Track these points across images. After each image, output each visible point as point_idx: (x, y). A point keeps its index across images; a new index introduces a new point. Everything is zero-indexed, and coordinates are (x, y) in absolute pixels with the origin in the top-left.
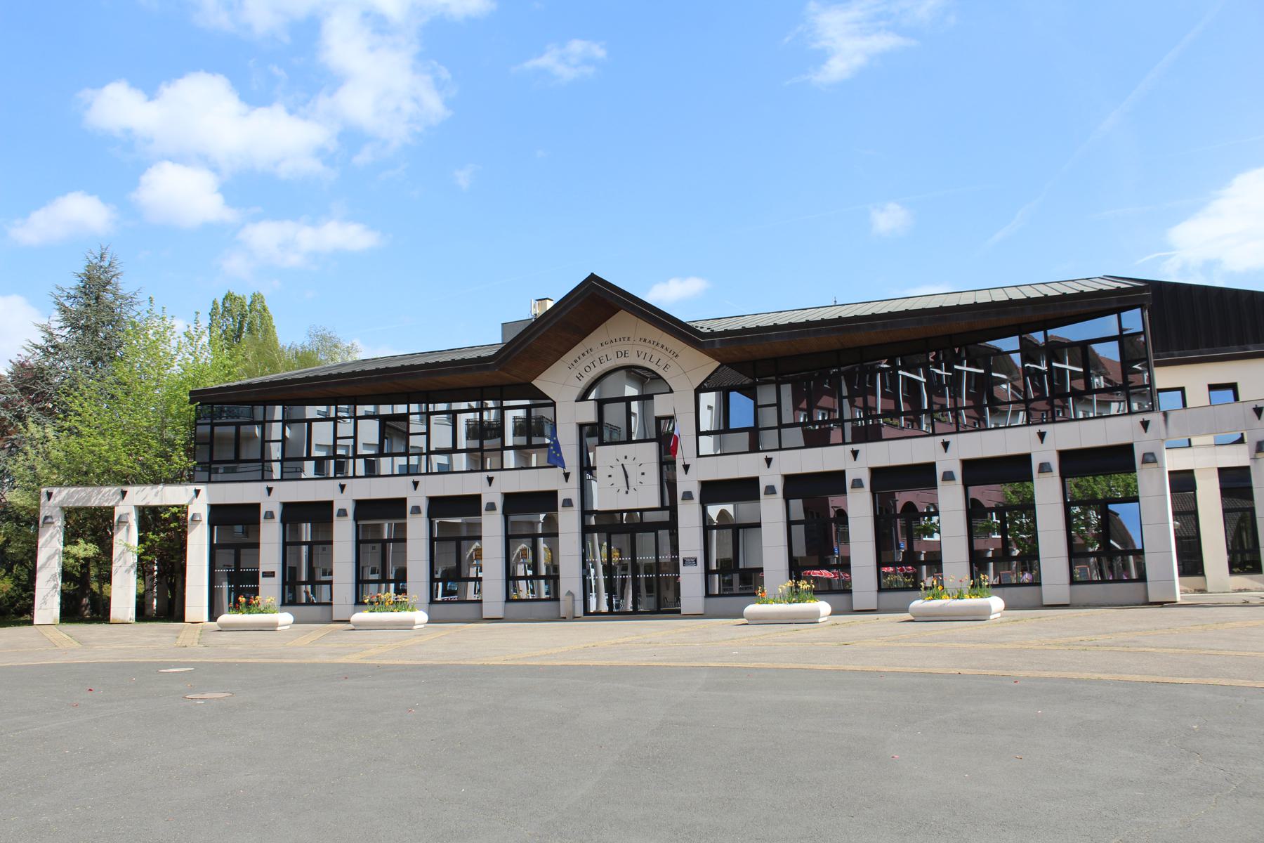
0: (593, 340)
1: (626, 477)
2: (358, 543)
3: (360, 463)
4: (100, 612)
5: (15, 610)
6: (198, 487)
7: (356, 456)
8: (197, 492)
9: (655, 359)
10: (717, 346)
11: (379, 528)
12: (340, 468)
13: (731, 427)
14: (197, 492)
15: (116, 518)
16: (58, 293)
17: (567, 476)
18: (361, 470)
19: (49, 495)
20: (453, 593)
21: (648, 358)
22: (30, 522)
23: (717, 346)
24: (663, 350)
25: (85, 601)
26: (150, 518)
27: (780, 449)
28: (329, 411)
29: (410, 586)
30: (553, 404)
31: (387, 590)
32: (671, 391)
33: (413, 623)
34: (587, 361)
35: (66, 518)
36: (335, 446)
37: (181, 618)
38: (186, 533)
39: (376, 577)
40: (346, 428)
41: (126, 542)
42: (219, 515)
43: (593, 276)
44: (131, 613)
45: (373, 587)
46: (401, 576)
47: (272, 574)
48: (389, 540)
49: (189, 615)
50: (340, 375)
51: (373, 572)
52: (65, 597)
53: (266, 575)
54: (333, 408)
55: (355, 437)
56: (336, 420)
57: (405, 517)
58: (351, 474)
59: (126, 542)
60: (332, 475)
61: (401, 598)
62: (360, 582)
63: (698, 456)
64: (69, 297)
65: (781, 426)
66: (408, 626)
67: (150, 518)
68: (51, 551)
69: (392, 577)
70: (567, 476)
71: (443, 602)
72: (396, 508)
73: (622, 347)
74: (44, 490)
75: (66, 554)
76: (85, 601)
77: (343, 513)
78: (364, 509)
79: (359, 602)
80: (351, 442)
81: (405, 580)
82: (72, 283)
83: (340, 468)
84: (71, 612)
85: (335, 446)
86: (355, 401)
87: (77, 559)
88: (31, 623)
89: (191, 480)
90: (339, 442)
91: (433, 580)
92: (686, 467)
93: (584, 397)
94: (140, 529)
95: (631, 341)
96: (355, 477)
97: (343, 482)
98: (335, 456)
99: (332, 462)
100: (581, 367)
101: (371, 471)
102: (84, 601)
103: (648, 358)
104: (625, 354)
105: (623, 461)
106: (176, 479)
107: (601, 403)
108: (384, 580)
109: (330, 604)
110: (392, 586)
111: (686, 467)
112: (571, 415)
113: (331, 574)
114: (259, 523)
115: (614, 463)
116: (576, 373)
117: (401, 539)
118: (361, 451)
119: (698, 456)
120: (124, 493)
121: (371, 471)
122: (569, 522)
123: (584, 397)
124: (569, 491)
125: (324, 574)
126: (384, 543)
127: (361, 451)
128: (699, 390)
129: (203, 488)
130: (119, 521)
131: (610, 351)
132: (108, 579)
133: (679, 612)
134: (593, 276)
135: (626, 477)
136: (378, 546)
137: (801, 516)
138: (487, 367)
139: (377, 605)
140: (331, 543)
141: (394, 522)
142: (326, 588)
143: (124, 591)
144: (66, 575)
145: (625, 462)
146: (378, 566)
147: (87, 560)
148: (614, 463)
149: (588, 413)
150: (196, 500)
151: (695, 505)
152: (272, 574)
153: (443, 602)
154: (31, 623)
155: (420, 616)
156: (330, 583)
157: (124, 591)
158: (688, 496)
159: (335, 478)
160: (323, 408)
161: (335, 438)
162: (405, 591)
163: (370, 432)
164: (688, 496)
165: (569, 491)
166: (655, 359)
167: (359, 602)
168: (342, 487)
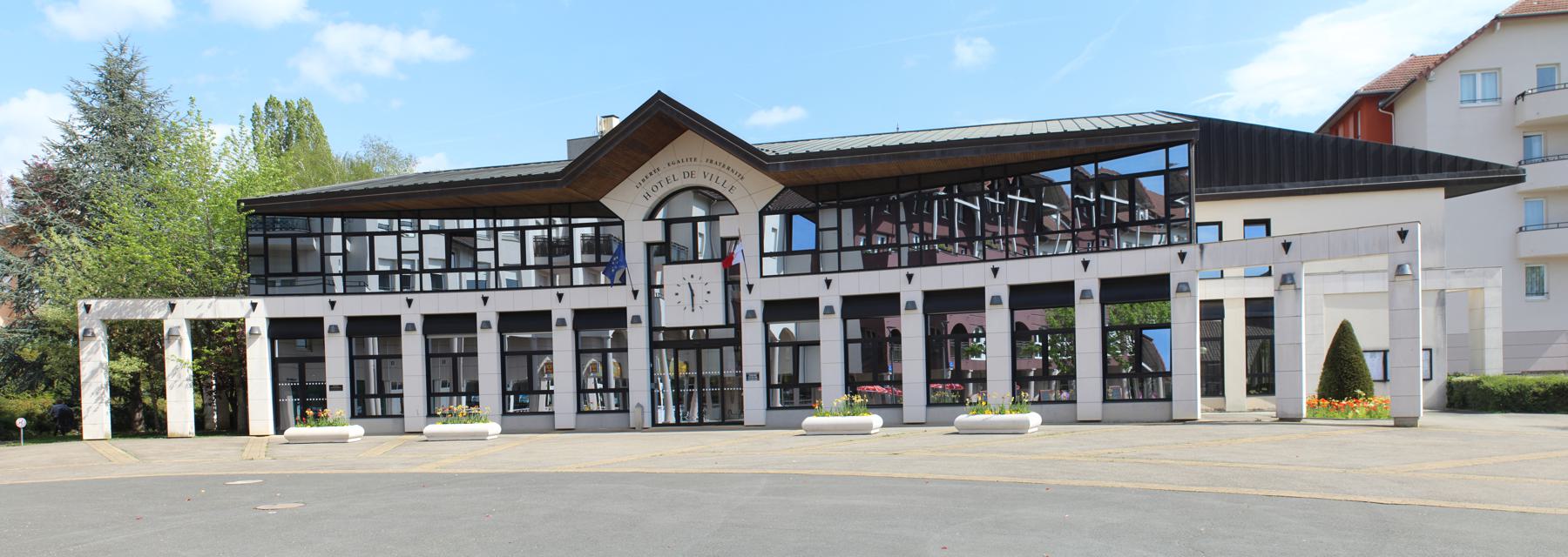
2: (428, 357)
3: (427, 277)
4: (156, 426)
5: (62, 423)
6: (255, 300)
7: (422, 271)
8: (254, 305)
9: (721, 181)
10: (782, 169)
11: (448, 343)
12: (406, 283)
14: (254, 305)
15: (166, 332)
16: (74, 86)
17: (635, 293)
18: (428, 285)
19: (88, 308)
20: (525, 405)
22: (67, 336)
23: (782, 169)
25: (139, 415)
26: (202, 331)
27: (840, 271)
28: (391, 225)
29: (482, 398)
30: (622, 223)
31: (459, 403)
33: (486, 434)
34: (654, 180)
35: (109, 332)
36: (400, 260)
37: (246, 432)
38: (245, 347)
39: (447, 390)
40: (410, 242)
41: (179, 358)
42: (280, 329)
44: (190, 427)
45: (444, 400)
46: (473, 390)
47: (340, 388)
48: (459, 355)
49: (254, 427)
50: (401, 188)
51: (444, 385)
52: (116, 413)
53: (333, 388)
54: (396, 222)
55: (420, 252)
56: (399, 234)
57: (550, 329)
58: (417, 288)
59: (179, 358)
60: (398, 289)
61: (474, 410)
62: (431, 395)
64: (87, 92)
65: (841, 249)
66: (481, 437)
67: (202, 331)
68: (96, 367)
69: (463, 390)
70: (635, 293)
71: (514, 414)
72: (466, 322)
74: (80, 303)
75: (113, 371)
76: (139, 415)
77: (411, 327)
78: (433, 323)
79: (431, 414)
80: (416, 257)
81: (477, 393)
82: (91, 79)
83: (406, 283)
84: (122, 425)
85: (400, 260)
86: (419, 215)
87: (124, 374)
88: (80, 438)
89: (246, 293)
90: (404, 256)
91: (505, 393)
92: (750, 287)
93: (651, 216)
94: (194, 343)
96: (422, 291)
97: (410, 296)
98: (401, 271)
99: (397, 277)
100: (648, 187)
101: (439, 286)
102: (137, 415)
104: (691, 175)
106: (230, 292)
107: (668, 223)
108: (456, 392)
109: (402, 416)
110: (464, 398)
111: (750, 287)
112: (639, 234)
113: (401, 387)
114: (399, 335)
115: (680, 281)
117: (471, 353)
118: (427, 266)
120: (172, 306)
121: (439, 286)
122: (637, 337)
123: (651, 216)
124: (637, 308)
125: (394, 387)
126: (455, 357)
127: (427, 266)
128: (764, 212)
129: (260, 301)
130: (169, 335)
131: (677, 171)
132: (163, 393)
136: (449, 360)
138: (555, 184)
139: (450, 416)
140: (400, 357)
141: (463, 336)
142: (396, 401)
143: (180, 405)
144: (115, 390)
146: (449, 379)
147: (136, 375)
148: (680, 281)
149: (655, 232)
150: (255, 314)
151: (836, 320)
152: (340, 388)
153: (514, 414)
154: (80, 438)
155: (493, 428)
156: (401, 396)
157: (180, 405)
158: (751, 314)
159: (401, 292)
160: (385, 222)
161: (400, 252)
162: (477, 404)
163: (435, 247)
164: (751, 314)
165: (637, 308)
167: (431, 414)
168: (410, 302)
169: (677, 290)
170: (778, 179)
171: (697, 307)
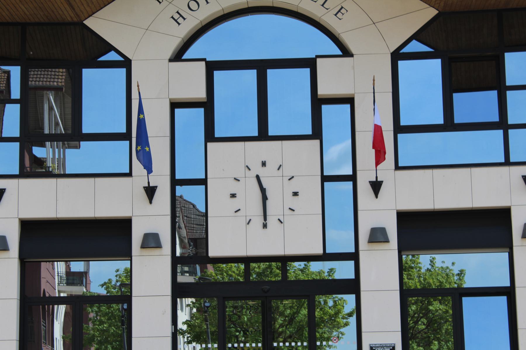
1: (265, 198)
13: (457, 120)
17: (150, 192)
30: (126, 63)
32: (346, 53)
70: (150, 192)
92: (376, 186)
93: (178, 56)
105: (257, 169)
107: (212, 67)
111: (376, 186)
115: (240, 173)
122: (151, 276)
124: (152, 219)
128: (397, 56)
135: (265, 198)
137: (291, 276)
148: (240, 173)
149: (190, 82)
158: (378, 236)
164: (378, 236)
165: (152, 219)
169: (234, 187)
171: (272, 221)
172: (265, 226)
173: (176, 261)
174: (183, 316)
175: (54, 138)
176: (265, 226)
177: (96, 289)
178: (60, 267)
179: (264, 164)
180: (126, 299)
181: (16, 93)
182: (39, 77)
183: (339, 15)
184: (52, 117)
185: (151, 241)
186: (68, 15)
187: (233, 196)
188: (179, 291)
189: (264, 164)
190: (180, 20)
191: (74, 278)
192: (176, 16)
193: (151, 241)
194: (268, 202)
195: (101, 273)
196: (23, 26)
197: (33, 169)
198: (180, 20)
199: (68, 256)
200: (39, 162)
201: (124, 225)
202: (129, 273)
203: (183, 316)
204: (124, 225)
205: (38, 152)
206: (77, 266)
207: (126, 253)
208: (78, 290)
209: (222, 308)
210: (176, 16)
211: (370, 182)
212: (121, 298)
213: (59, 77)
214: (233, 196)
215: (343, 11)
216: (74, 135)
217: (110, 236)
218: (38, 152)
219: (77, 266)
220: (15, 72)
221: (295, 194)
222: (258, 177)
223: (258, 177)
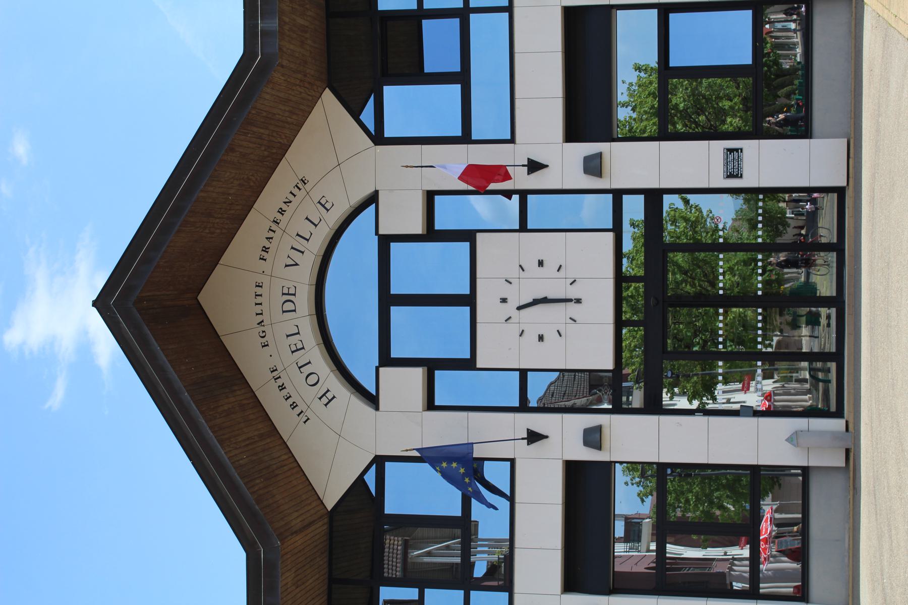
0: (254, 365)
1: (545, 300)
9: (306, 229)
13: (457, 68)
17: (533, 437)
21: (300, 244)
23: (274, 24)
24: (289, 210)
30: (379, 462)
32: (373, 199)
34: (295, 380)
43: (95, 304)
63: (512, 140)
70: (533, 437)
73: (273, 300)
92: (534, 166)
93: (373, 400)
95: (265, 280)
100: (307, 395)
103: (300, 244)
104: (289, 295)
107: (386, 359)
111: (534, 166)
112: (402, 420)
115: (514, 329)
116: (318, 405)
119: (512, 140)
122: (634, 439)
123: (373, 400)
128: (378, 138)
133: (840, 192)
134: (95, 304)
135: (545, 300)
145: (513, 303)
158: (593, 166)
164: (593, 166)
165: (566, 435)
166: (306, 229)
170: (301, 112)
171: (572, 293)
172: (578, 301)
173: (618, 409)
174: (682, 403)
175: (466, 552)
176: (578, 301)
177: (646, 508)
178: (620, 549)
179: (504, 300)
180: (662, 469)
181: (411, 594)
182: (392, 566)
183: (328, 206)
184: (440, 552)
185: (593, 438)
186: (321, 528)
187: (541, 338)
188: (653, 406)
189: (504, 300)
190: (329, 395)
191: (633, 533)
192: (325, 400)
193: (593, 438)
194: (550, 297)
195: (629, 500)
196: (333, 581)
197: (502, 576)
198: (329, 395)
199: (608, 540)
200: (492, 570)
201: (572, 469)
202: (632, 466)
203: (682, 403)
204: (572, 469)
205: (480, 570)
206: (619, 529)
207: (607, 468)
208: (647, 526)
209: (676, 355)
210: (325, 400)
211: (528, 174)
212: (660, 476)
213: (393, 543)
214: (541, 338)
215: (323, 202)
216: (463, 526)
217: (586, 487)
218: (480, 570)
219: (619, 529)
220: (386, 593)
221: (541, 263)
222: (519, 308)
223: (519, 308)
